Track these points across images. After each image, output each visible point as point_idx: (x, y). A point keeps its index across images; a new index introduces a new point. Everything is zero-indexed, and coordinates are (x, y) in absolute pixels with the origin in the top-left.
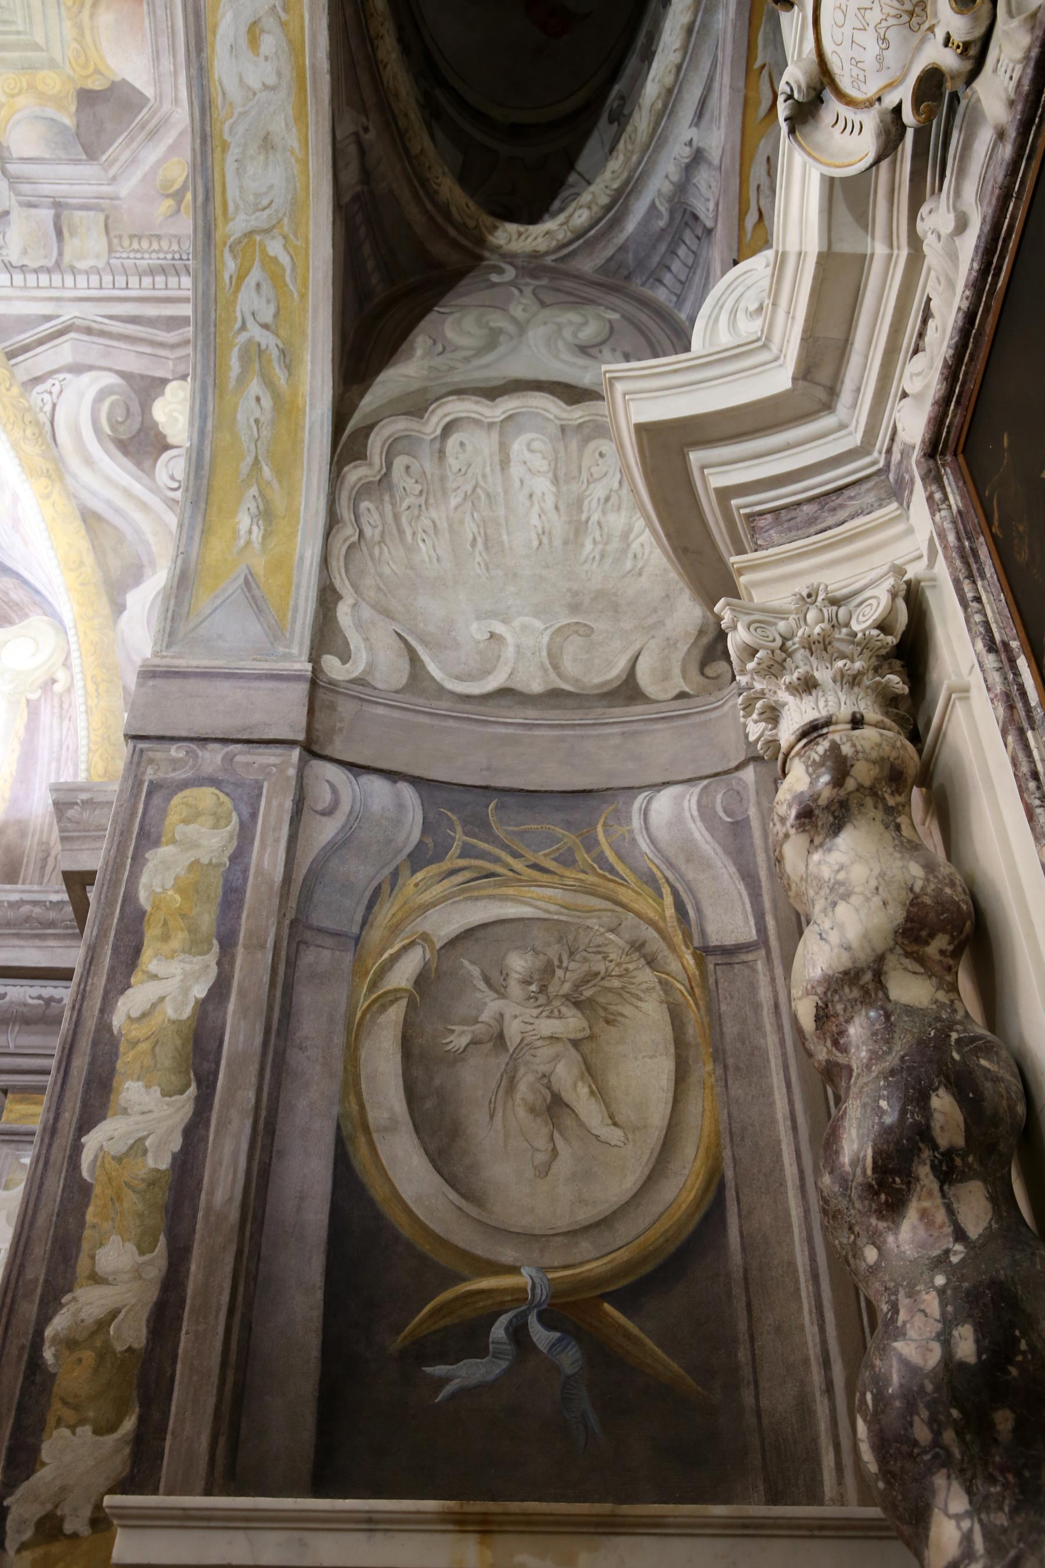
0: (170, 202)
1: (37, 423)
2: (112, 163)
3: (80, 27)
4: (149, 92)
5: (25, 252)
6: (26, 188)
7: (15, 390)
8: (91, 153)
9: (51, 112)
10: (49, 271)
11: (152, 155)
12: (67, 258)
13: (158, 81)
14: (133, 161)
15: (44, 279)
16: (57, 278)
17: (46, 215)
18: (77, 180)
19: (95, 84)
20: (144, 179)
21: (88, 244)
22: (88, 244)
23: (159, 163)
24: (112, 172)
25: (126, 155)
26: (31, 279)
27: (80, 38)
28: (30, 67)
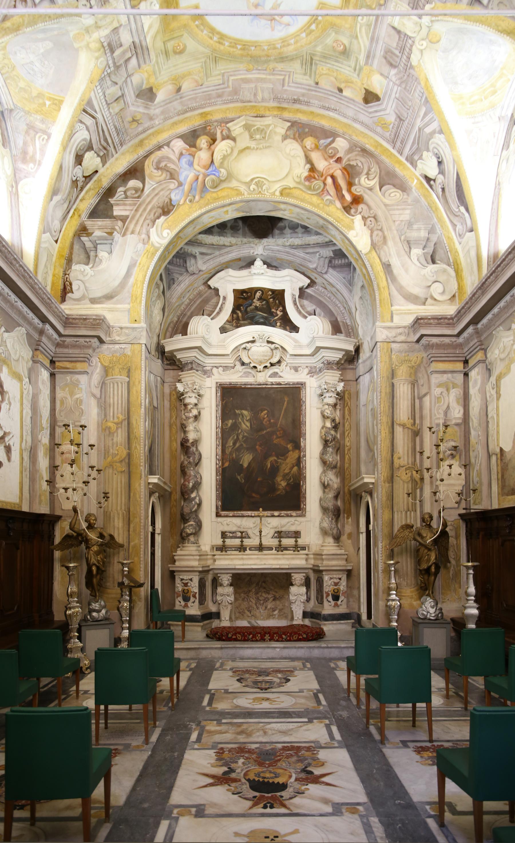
0: (131, 119)
1: (72, 131)
2: (137, 102)
3: (167, 81)
4: (156, 102)
5: (109, 94)
6: (125, 85)
7: (77, 119)
8: (138, 96)
9: (145, 82)
10: (107, 103)
11: (141, 110)
12: (111, 105)
13: (159, 103)
14: (138, 106)
15: (104, 103)
16: (106, 106)
17: (120, 94)
18: (130, 96)
19: (154, 90)
20: (135, 111)
21: (116, 108)
22: (116, 108)
23: (140, 112)
24: (135, 103)
25: (139, 104)
26: (104, 100)
27: (164, 82)
28: (154, 73)
